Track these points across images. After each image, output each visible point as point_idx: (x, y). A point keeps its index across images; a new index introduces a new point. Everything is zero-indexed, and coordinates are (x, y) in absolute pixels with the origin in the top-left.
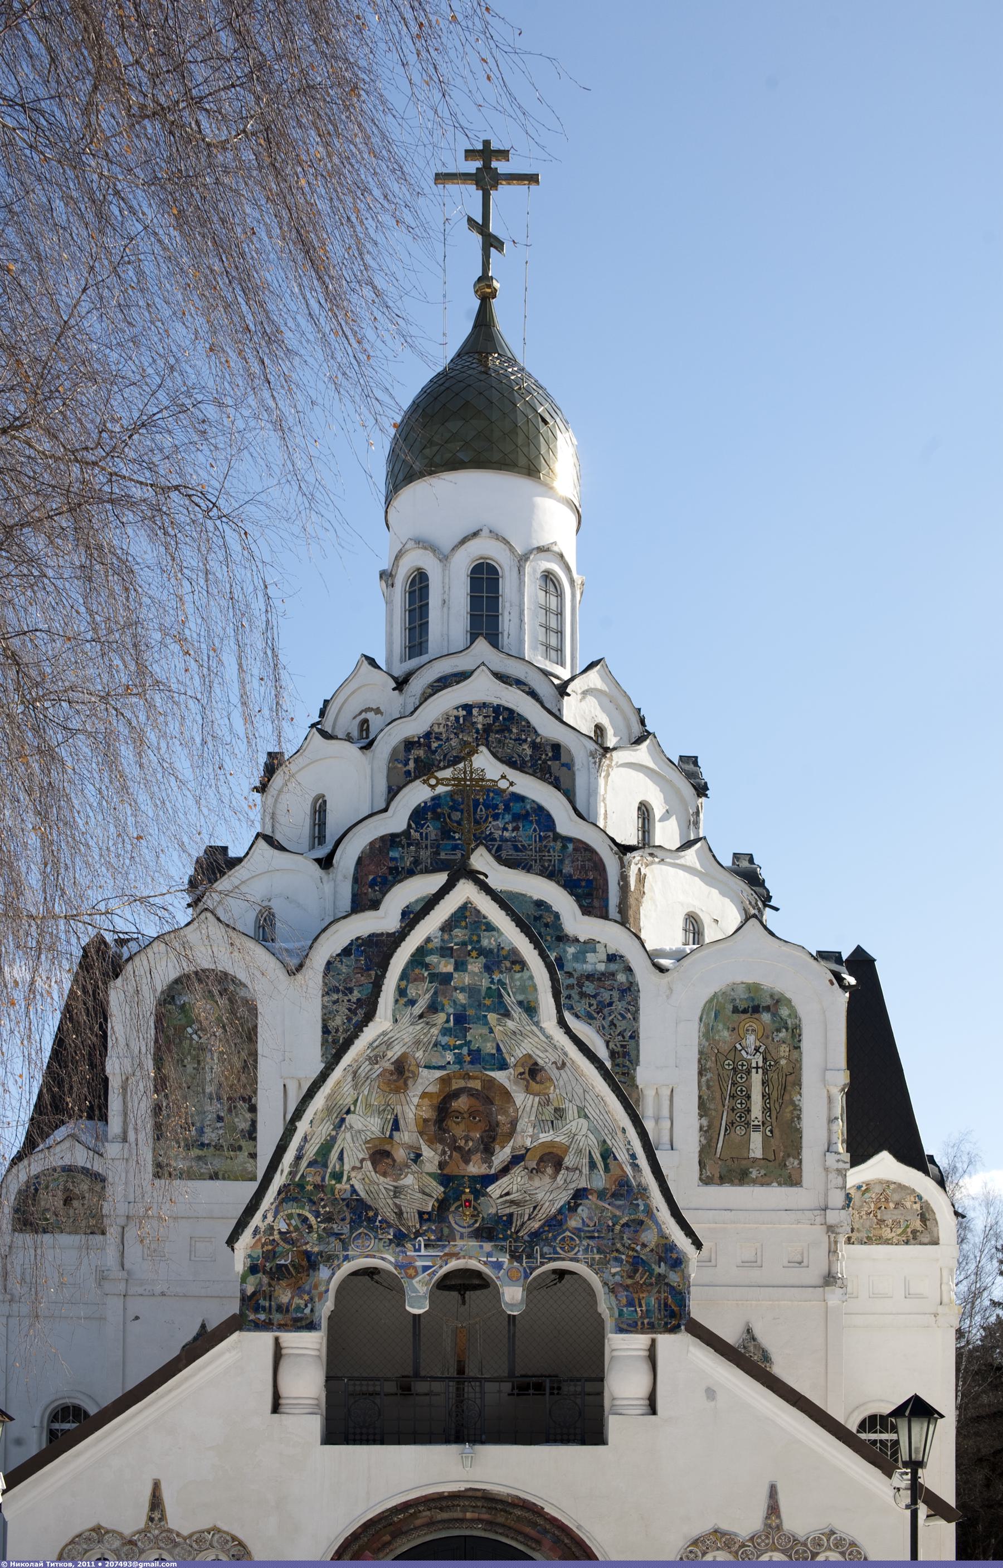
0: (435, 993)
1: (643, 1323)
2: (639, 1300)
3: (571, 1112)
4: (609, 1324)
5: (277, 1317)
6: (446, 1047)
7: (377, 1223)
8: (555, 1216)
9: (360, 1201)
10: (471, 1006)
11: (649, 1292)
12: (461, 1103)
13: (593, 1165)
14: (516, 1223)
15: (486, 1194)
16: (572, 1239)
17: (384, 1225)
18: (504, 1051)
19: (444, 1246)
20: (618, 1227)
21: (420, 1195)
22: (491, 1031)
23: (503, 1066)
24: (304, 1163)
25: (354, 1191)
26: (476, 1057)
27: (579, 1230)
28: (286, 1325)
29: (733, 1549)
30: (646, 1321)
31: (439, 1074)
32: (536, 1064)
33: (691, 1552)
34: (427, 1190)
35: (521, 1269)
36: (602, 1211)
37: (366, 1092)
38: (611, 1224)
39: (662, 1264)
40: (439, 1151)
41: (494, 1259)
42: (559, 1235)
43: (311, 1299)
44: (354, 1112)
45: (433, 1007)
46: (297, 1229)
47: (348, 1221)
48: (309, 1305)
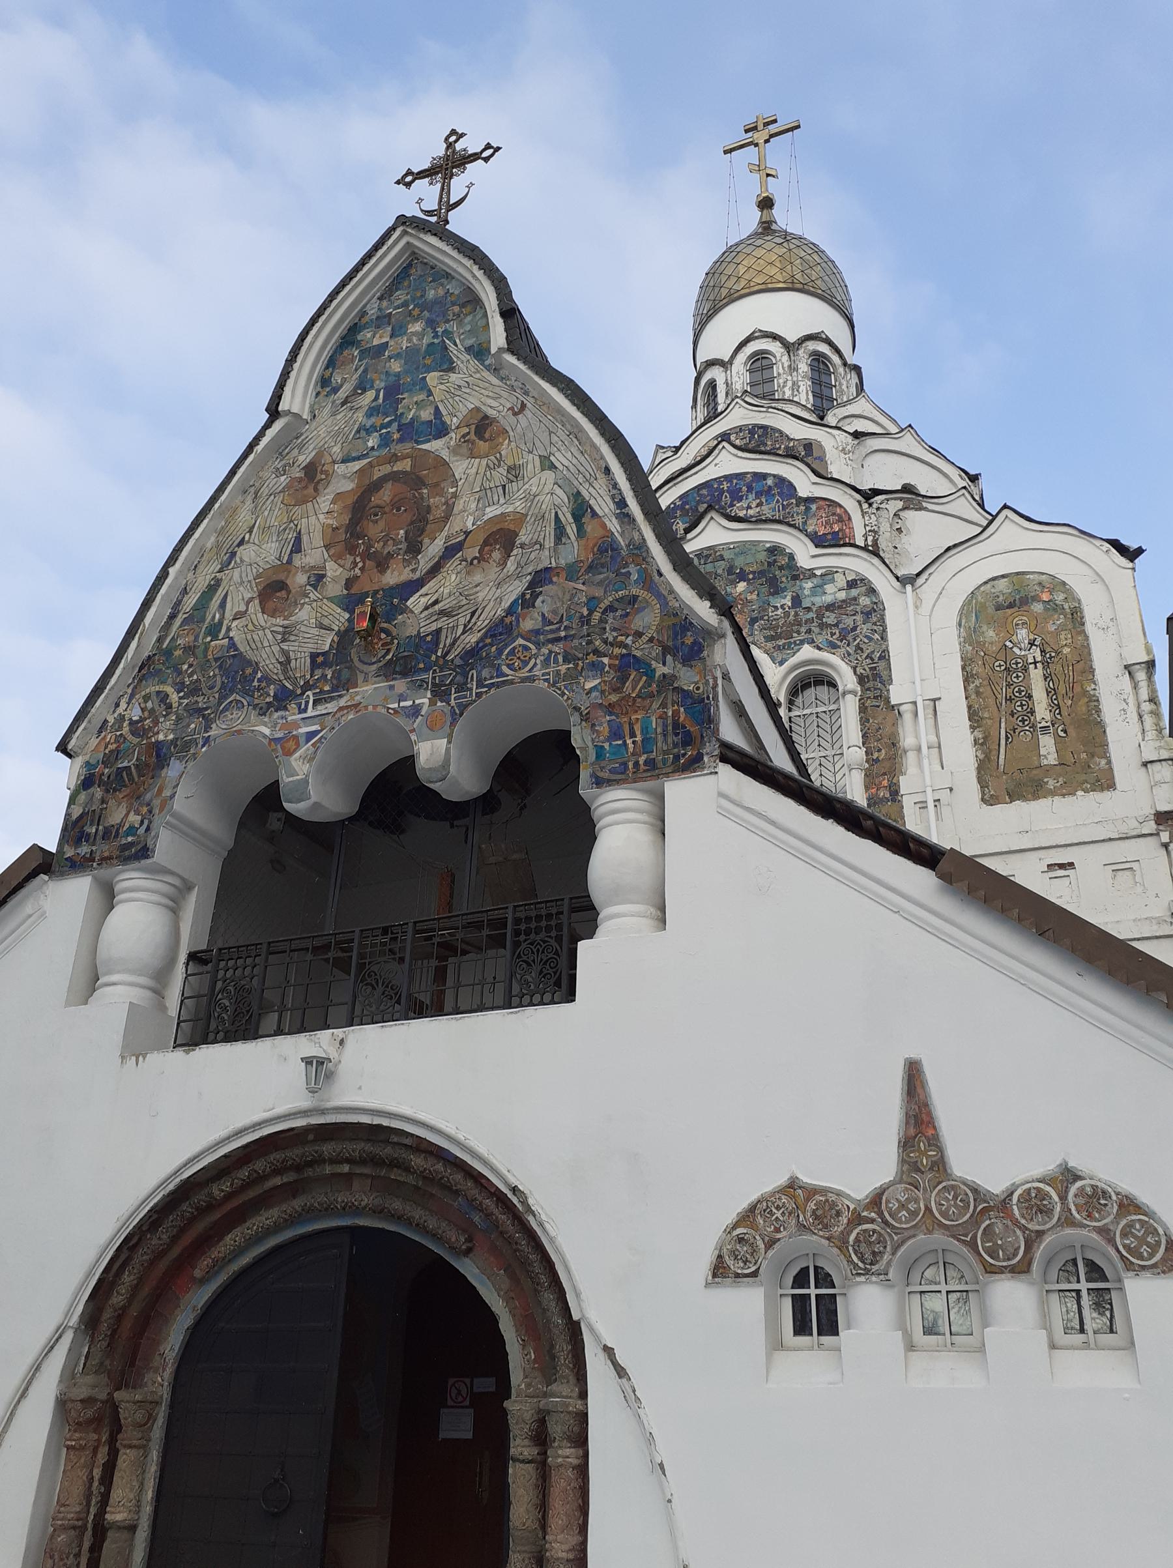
0: (365, 371)
1: (636, 764)
2: (631, 725)
3: (530, 466)
4: (584, 775)
5: (103, 849)
6: (368, 432)
7: (256, 683)
8: (502, 620)
9: (239, 656)
10: (406, 372)
11: (646, 709)
12: (385, 495)
13: (560, 532)
14: (446, 640)
15: (405, 610)
16: (526, 648)
17: (264, 684)
18: (444, 412)
19: (340, 696)
20: (597, 616)
21: (315, 631)
22: (430, 394)
23: (440, 430)
24: (178, 622)
25: (232, 645)
26: (411, 431)
27: (537, 632)
28: (110, 858)
29: (837, 1230)
30: (642, 759)
31: (356, 466)
32: (486, 417)
33: (741, 1240)
34: (326, 622)
35: (447, 709)
36: (573, 596)
37: (266, 513)
38: (586, 613)
39: (669, 658)
40: (348, 566)
41: (410, 703)
42: (506, 646)
43: (150, 812)
44: (248, 542)
45: (362, 387)
46: (152, 711)
47: (216, 689)
48: (146, 822)
